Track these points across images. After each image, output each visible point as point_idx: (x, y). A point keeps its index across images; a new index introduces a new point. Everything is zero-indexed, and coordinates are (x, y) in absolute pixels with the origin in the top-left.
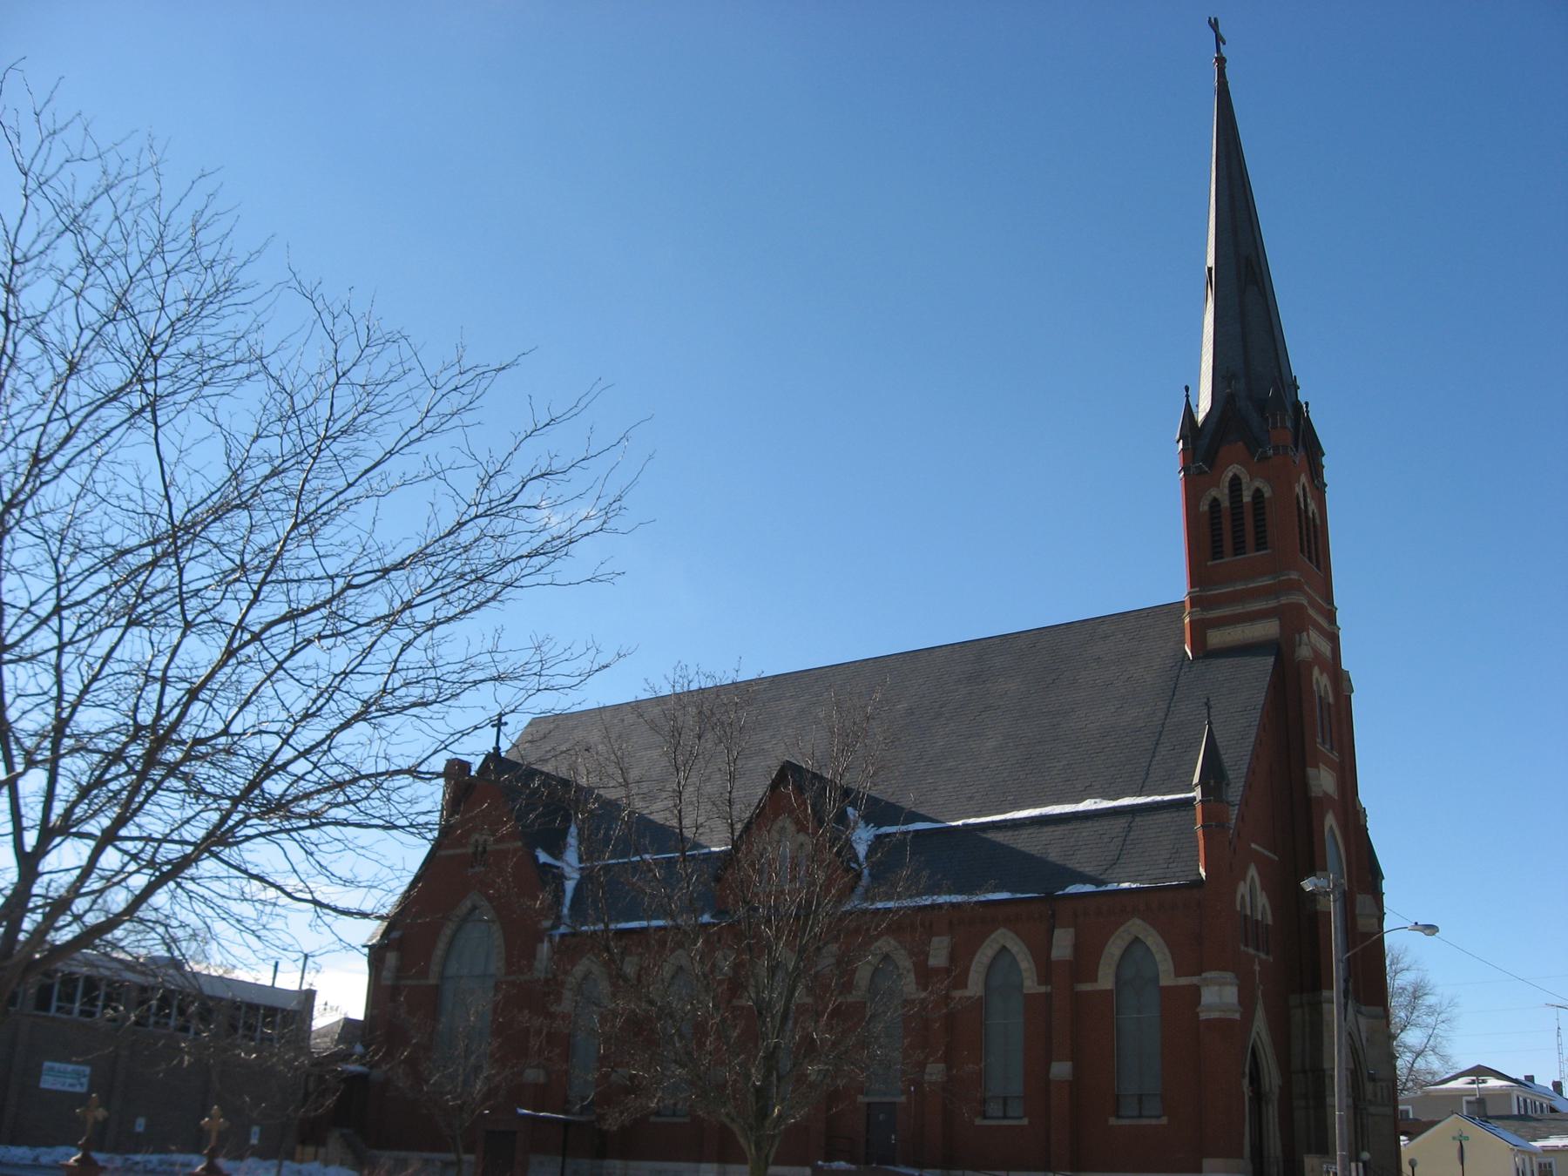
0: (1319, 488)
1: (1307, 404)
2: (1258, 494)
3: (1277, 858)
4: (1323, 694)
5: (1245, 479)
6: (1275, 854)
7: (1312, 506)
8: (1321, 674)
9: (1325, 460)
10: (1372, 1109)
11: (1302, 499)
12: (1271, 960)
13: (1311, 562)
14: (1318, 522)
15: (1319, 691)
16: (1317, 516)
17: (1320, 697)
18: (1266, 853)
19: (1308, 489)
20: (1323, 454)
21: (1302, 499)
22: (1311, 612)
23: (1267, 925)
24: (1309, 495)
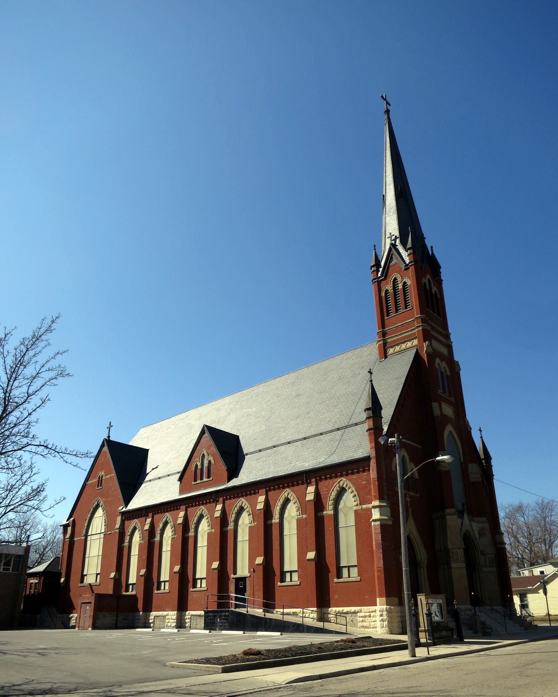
0: (439, 282)
1: (432, 247)
2: (405, 284)
3: (420, 447)
4: (443, 370)
5: (399, 279)
6: (420, 445)
7: (434, 289)
8: (442, 361)
9: (441, 270)
10: (485, 569)
11: (427, 285)
12: (418, 495)
13: (434, 312)
14: (439, 296)
15: (440, 369)
16: (438, 293)
17: (442, 373)
18: (413, 444)
19: (431, 281)
20: (440, 267)
21: (427, 285)
22: (432, 332)
23: (415, 479)
24: (432, 284)
